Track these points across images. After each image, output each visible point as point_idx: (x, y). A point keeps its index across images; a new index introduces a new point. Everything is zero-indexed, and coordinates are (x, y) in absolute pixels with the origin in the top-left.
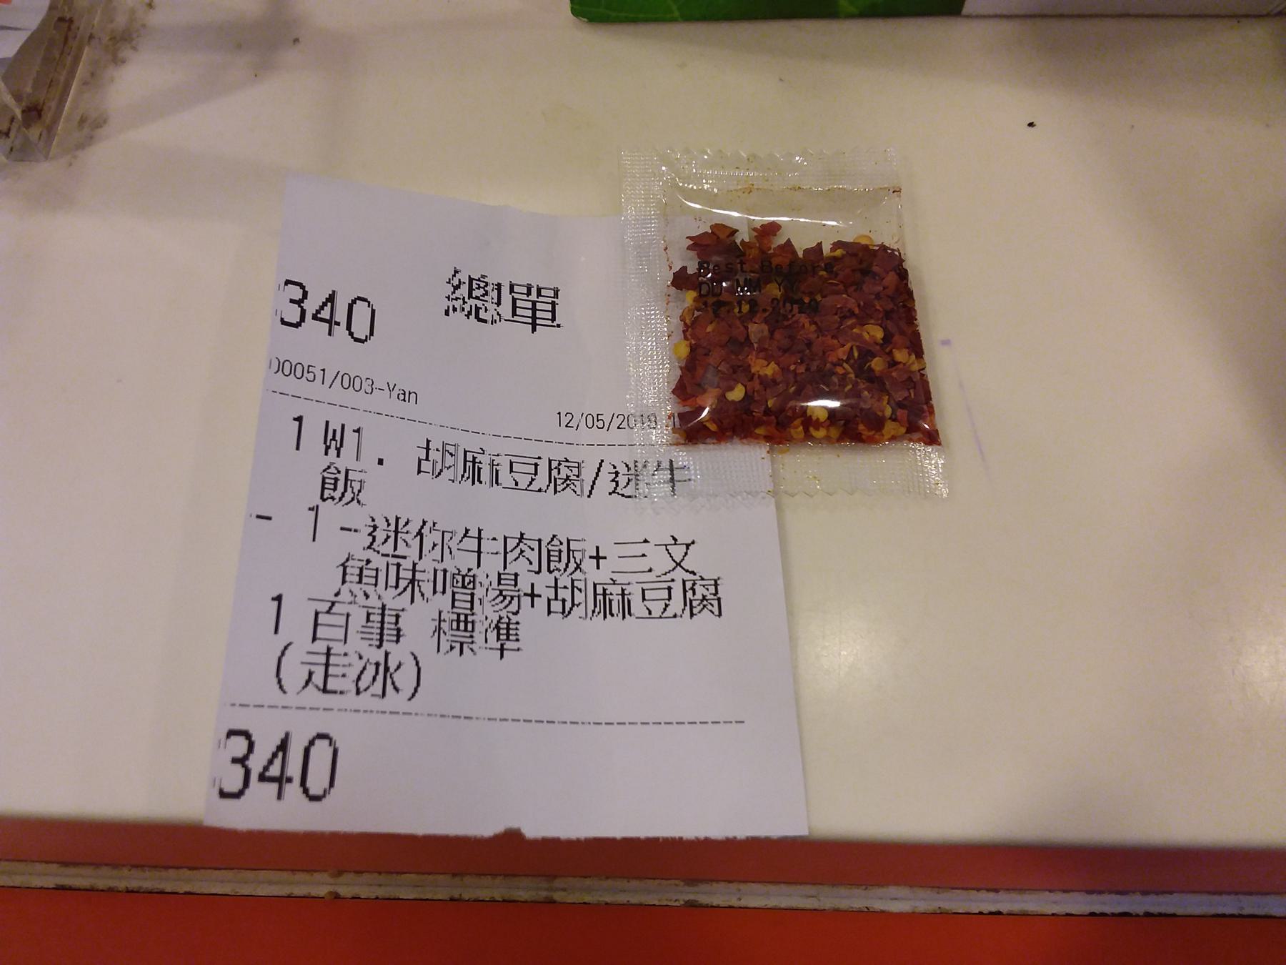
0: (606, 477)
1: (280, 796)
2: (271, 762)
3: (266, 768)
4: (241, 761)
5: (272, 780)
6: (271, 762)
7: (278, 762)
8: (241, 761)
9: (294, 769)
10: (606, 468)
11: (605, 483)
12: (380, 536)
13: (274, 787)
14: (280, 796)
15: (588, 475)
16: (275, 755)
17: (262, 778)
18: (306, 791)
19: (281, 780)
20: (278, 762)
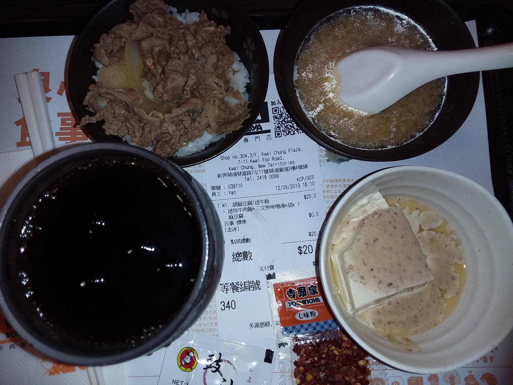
0: (254, 202)
1: (229, 309)
2: (227, 305)
3: (227, 306)
4: (224, 305)
5: (228, 307)
6: (227, 305)
7: (228, 305)
8: (224, 305)
9: (230, 306)
10: (254, 201)
11: (254, 203)
12: (230, 211)
13: (228, 308)
14: (229, 309)
15: (252, 202)
16: (227, 304)
17: (227, 307)
18: (232, 308)
19: (229, 307)
20: (228, 305)
